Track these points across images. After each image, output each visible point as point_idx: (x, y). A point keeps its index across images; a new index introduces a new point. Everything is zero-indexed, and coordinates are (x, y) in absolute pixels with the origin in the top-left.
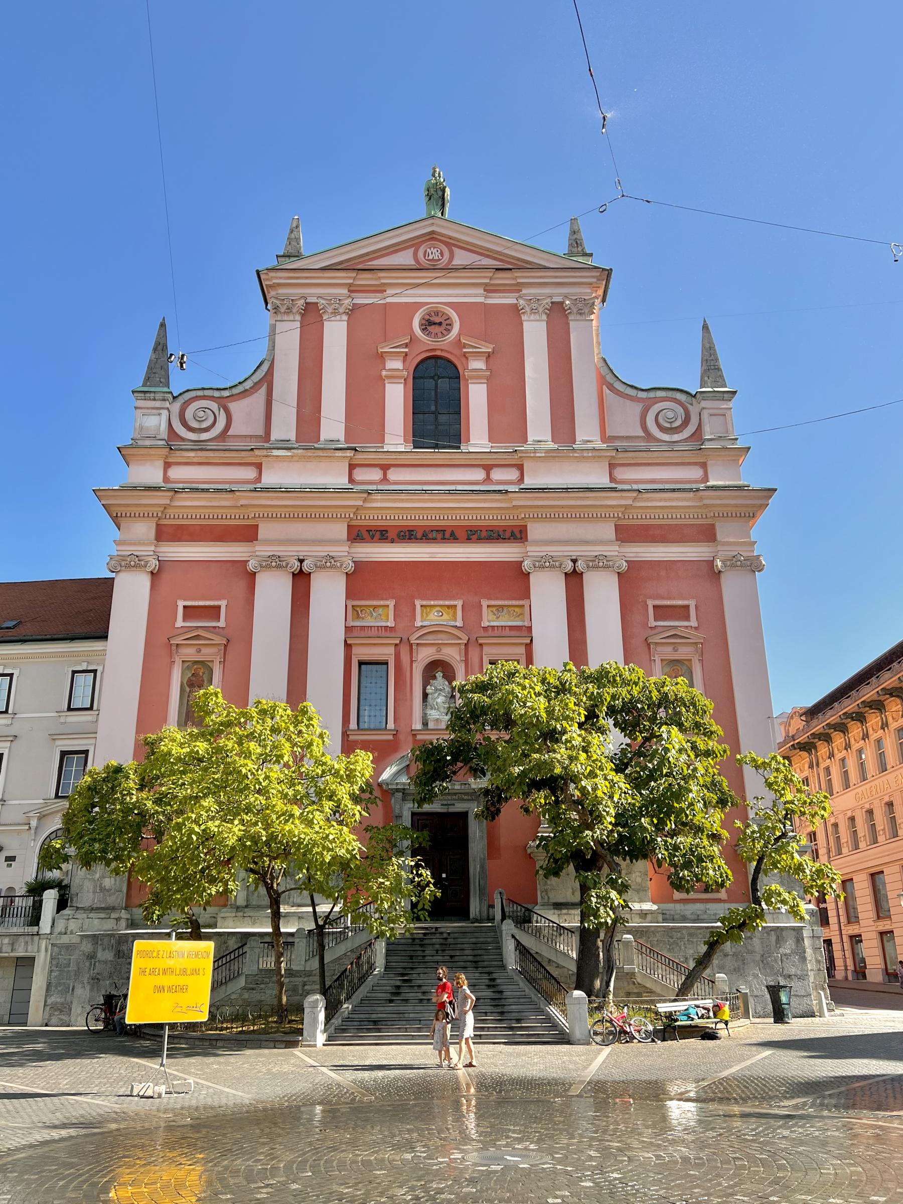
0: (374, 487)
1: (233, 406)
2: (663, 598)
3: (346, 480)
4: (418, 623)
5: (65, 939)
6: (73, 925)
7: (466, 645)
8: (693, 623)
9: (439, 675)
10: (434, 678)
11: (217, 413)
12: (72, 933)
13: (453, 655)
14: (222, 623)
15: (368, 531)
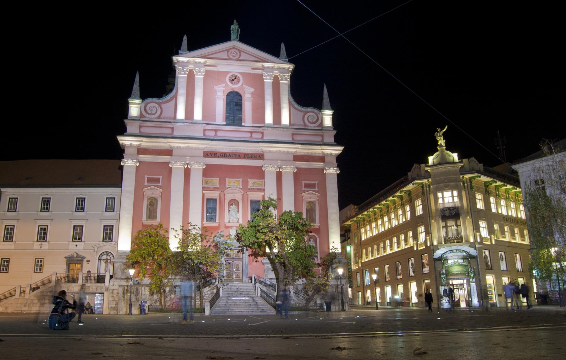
0: (212, 138)
1: (163, 106)
2: (307, 181)
3: (203, 135)
4: (227, 187)
5: (114, 288)
6: (116, 283)
7: (243, 194)
8: (317, 189)
9: (234, 204)
10: (232, 205)
11: (157, 107)
12: (116, 285)
13: (239, 197)
14: (160, 184)
15: (211, 153)
